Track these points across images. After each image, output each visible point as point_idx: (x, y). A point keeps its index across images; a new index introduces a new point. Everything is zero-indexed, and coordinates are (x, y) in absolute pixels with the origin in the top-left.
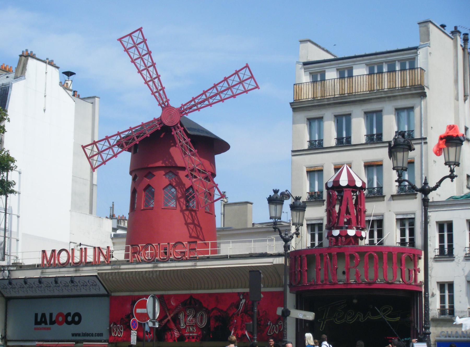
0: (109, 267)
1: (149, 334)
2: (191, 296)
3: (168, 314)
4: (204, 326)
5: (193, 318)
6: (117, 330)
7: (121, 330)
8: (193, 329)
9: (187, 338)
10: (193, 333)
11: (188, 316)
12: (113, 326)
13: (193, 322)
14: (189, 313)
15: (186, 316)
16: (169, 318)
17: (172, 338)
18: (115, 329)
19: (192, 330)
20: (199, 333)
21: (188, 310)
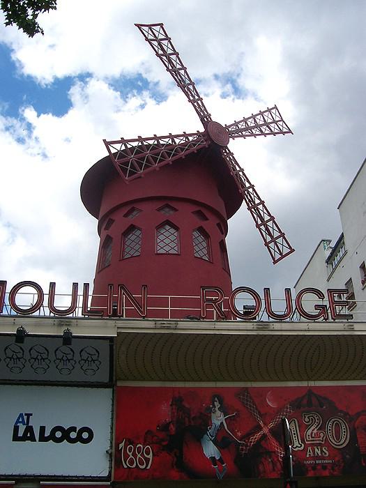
0: (151, 324)
1: (218, 463)
2: (310, 391)
3: (261, 423)
4: (344, 445)
5: (320, 429)
6: (135, 455)
7: (146, 456)
8: (322, 451)
9: (310, 469)
10: (324, 458)
11: (308, 427)
12: (126, 446)
13: (321, 439)
14: (308, 422)
15: (303, 428)
16: (265, 430)
17: (276, 470)
18: (130, 454)
19: (319, 452)
20: (337, 459)
21: (307, 416)
